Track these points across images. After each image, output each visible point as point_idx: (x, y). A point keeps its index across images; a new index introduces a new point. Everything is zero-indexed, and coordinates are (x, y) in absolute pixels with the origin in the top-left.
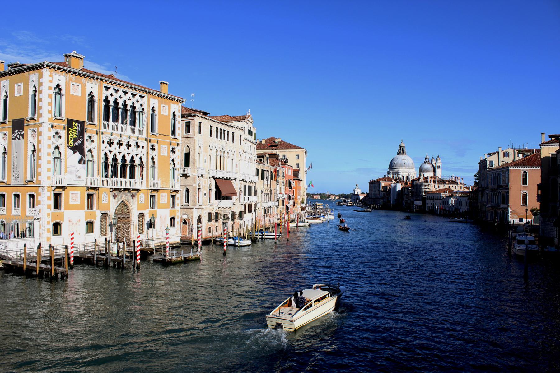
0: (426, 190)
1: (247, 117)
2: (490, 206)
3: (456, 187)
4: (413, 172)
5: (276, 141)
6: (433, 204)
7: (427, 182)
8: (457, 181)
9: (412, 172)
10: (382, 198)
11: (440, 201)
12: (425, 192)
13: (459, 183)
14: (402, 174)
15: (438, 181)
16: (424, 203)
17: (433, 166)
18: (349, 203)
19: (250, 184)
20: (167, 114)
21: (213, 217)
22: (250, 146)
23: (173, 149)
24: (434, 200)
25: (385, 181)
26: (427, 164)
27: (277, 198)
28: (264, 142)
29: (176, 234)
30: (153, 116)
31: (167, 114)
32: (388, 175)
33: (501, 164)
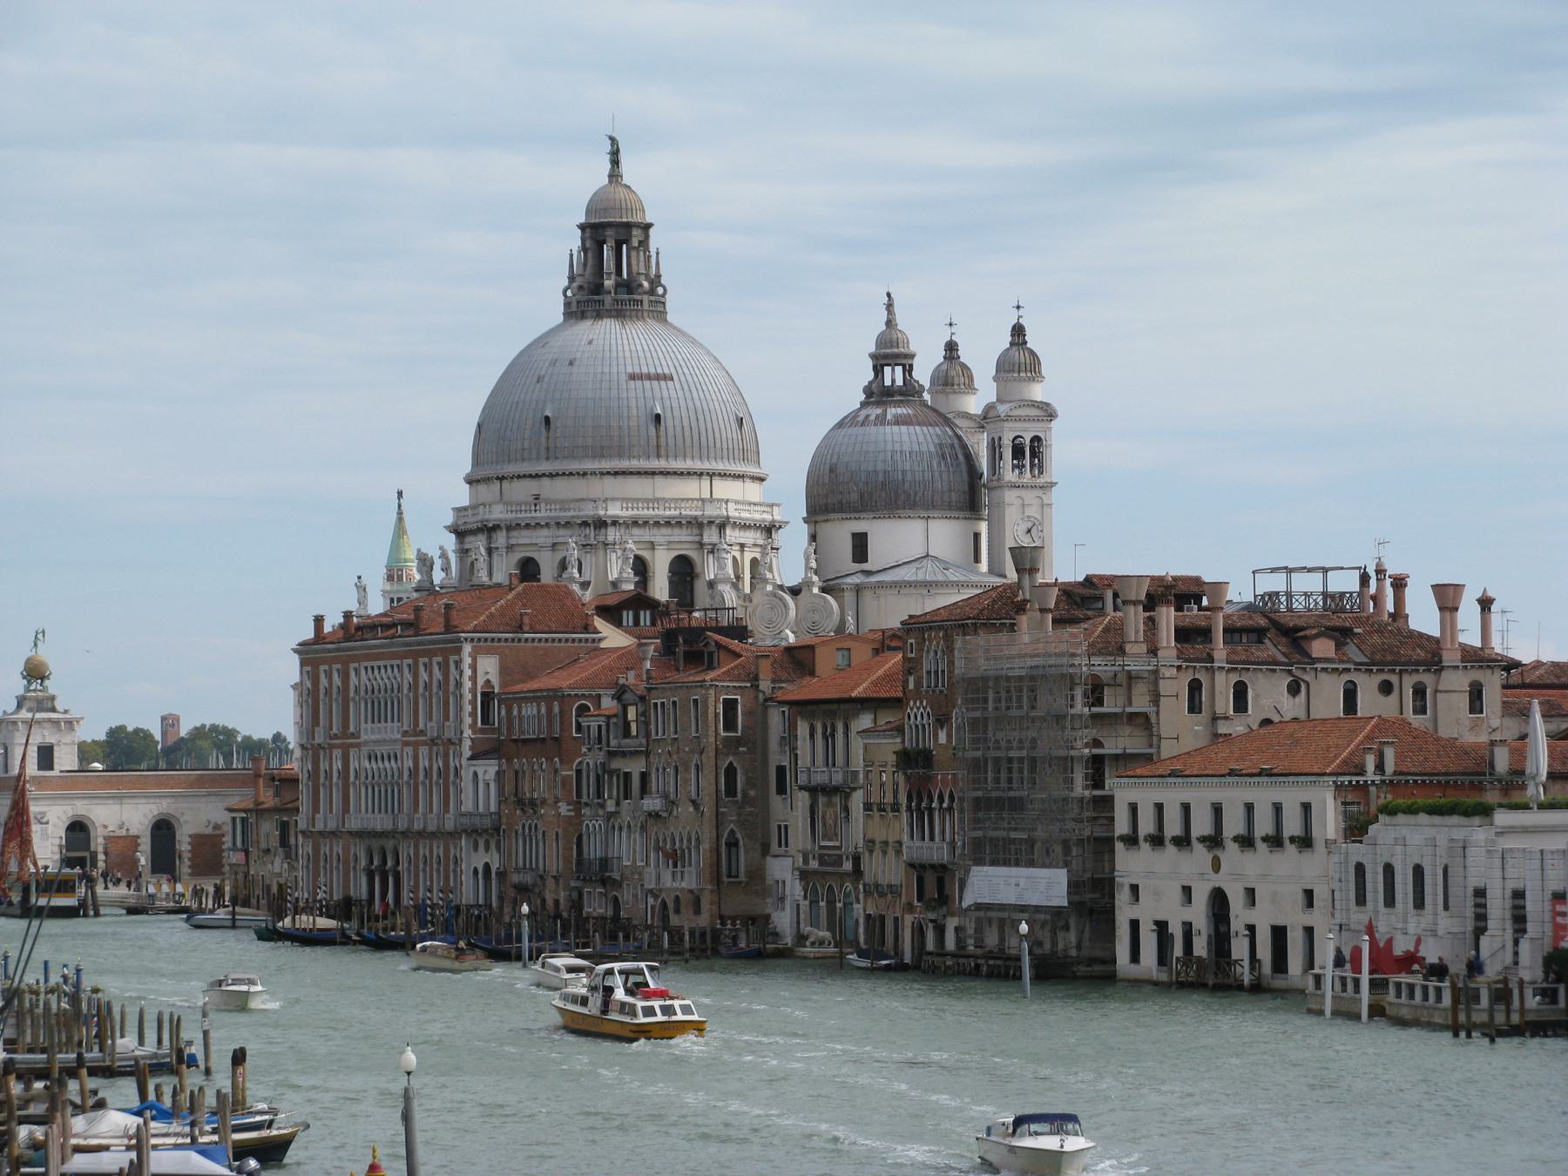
3: (1420, 692)
4: (747, 515)
6: (1219, 900)
7: (1114, 644)
8: (1423, 617)
9: (733, 511)
10: (489, 832)
11: (1315, 869)
13: (1450, 657)
26: (898, 421)
32: (463, 552)
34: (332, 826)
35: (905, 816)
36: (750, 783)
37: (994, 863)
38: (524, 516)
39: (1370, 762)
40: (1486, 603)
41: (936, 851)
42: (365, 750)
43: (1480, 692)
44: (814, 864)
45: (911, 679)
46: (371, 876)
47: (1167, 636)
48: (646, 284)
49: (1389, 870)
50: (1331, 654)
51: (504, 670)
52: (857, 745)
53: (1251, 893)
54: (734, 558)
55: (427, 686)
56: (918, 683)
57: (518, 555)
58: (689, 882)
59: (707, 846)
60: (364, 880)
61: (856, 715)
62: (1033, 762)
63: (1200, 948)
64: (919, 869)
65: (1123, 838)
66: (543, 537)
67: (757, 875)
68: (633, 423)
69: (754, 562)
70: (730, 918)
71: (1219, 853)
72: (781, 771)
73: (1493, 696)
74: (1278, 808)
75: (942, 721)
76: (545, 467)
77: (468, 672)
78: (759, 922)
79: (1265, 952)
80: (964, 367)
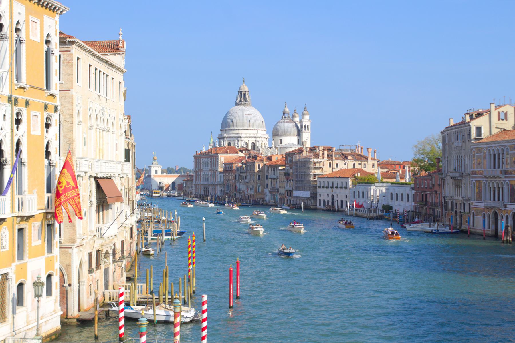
0: (315, 171)
1: (121, 45)
2: (483, 204)
3: (365, 165)
6: (333, 196)
7: (317, 156)
9: (262, 136)
11: (347, 191)
12: (315, 175)
13: (369, 159)
14: (246, 140)
16: (314, 196)
17: (296, 125)
18: (155, 193)
20: (38, 39)
23: (47, 118)
24: (334, 189)
25: (227, 153)
26: (287, 122)
29: (55, 311)
30: (20, 42)
31: (38, 39)
32: (220, 142)
33: (495, 131)
34: (198, 183)
35: (285, 183)
36: (262, 177)
37: (299, 190)
39: (356, 175)
40: (375, 152)
41: (290, 189)
42: (203, 172)
44: (271, 190)
45: (286, 162)
46: (204, 191)
48: (248, 101)
49: (359, 192)
50: (351, 159)
51: (225, 160)
52: (278, 172)
54: (261, 143)
55: (213, 162)
56: (287, 162)
58: (253, 192)
59: (255, 187)
60: (203, 192)
62: (305, 175)
63: (330, 204)
64: (287, 191)
65: (318, 187)
66: (232, 139)
67: (263, 192)
68: (246, 122)
69: (264, 144)
70: (259, 198)
71: (333, 189)
72: (267, 176)
73: (376, 165)
74: (342, 182)
75: (291, 168)
77: (219, 160)
78: (263, 199)
79: (340, 204)
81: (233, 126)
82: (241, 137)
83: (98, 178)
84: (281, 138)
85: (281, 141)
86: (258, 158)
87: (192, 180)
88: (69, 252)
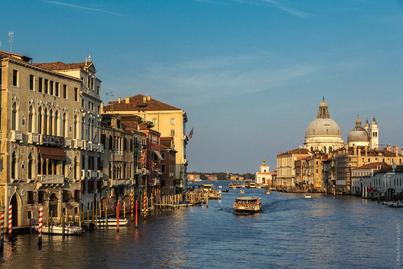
1: (86, 65)
4: (339, 141)
5: (145, 99)
6: (361, 183)
7: (353, 154)
13: (397, 155)
14: (325, 145)
15: (368, 153)
18: (251, 185)
19: (92, 155)
21: (36, 197)
22: (91, 104)
26: (359, 130)
27: (135, 174)
28: (127, 101)
36: (320, 171)
38: (311, 142)
39: (378, 167)
43: (401, 160)
44: (326, 181)
47: (359, 152)
51: (297, 159)
53: (364, 183)
57: (310, 147)
61: (329, 163)
63: (360, 190)
66: (313, 144)
76: (314, 136)
77: (293, 159)
80: (368, 124)
81: (314, 134)
82: (320, 143)
83: (38, 145)
84: (354, 143)
85: (354, 145)
86: (317, 156)
87: (276, 175)
88: (4, 188)
